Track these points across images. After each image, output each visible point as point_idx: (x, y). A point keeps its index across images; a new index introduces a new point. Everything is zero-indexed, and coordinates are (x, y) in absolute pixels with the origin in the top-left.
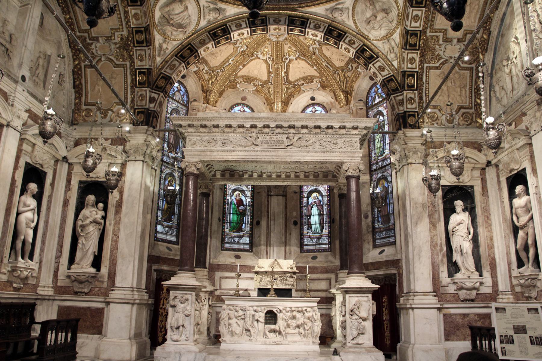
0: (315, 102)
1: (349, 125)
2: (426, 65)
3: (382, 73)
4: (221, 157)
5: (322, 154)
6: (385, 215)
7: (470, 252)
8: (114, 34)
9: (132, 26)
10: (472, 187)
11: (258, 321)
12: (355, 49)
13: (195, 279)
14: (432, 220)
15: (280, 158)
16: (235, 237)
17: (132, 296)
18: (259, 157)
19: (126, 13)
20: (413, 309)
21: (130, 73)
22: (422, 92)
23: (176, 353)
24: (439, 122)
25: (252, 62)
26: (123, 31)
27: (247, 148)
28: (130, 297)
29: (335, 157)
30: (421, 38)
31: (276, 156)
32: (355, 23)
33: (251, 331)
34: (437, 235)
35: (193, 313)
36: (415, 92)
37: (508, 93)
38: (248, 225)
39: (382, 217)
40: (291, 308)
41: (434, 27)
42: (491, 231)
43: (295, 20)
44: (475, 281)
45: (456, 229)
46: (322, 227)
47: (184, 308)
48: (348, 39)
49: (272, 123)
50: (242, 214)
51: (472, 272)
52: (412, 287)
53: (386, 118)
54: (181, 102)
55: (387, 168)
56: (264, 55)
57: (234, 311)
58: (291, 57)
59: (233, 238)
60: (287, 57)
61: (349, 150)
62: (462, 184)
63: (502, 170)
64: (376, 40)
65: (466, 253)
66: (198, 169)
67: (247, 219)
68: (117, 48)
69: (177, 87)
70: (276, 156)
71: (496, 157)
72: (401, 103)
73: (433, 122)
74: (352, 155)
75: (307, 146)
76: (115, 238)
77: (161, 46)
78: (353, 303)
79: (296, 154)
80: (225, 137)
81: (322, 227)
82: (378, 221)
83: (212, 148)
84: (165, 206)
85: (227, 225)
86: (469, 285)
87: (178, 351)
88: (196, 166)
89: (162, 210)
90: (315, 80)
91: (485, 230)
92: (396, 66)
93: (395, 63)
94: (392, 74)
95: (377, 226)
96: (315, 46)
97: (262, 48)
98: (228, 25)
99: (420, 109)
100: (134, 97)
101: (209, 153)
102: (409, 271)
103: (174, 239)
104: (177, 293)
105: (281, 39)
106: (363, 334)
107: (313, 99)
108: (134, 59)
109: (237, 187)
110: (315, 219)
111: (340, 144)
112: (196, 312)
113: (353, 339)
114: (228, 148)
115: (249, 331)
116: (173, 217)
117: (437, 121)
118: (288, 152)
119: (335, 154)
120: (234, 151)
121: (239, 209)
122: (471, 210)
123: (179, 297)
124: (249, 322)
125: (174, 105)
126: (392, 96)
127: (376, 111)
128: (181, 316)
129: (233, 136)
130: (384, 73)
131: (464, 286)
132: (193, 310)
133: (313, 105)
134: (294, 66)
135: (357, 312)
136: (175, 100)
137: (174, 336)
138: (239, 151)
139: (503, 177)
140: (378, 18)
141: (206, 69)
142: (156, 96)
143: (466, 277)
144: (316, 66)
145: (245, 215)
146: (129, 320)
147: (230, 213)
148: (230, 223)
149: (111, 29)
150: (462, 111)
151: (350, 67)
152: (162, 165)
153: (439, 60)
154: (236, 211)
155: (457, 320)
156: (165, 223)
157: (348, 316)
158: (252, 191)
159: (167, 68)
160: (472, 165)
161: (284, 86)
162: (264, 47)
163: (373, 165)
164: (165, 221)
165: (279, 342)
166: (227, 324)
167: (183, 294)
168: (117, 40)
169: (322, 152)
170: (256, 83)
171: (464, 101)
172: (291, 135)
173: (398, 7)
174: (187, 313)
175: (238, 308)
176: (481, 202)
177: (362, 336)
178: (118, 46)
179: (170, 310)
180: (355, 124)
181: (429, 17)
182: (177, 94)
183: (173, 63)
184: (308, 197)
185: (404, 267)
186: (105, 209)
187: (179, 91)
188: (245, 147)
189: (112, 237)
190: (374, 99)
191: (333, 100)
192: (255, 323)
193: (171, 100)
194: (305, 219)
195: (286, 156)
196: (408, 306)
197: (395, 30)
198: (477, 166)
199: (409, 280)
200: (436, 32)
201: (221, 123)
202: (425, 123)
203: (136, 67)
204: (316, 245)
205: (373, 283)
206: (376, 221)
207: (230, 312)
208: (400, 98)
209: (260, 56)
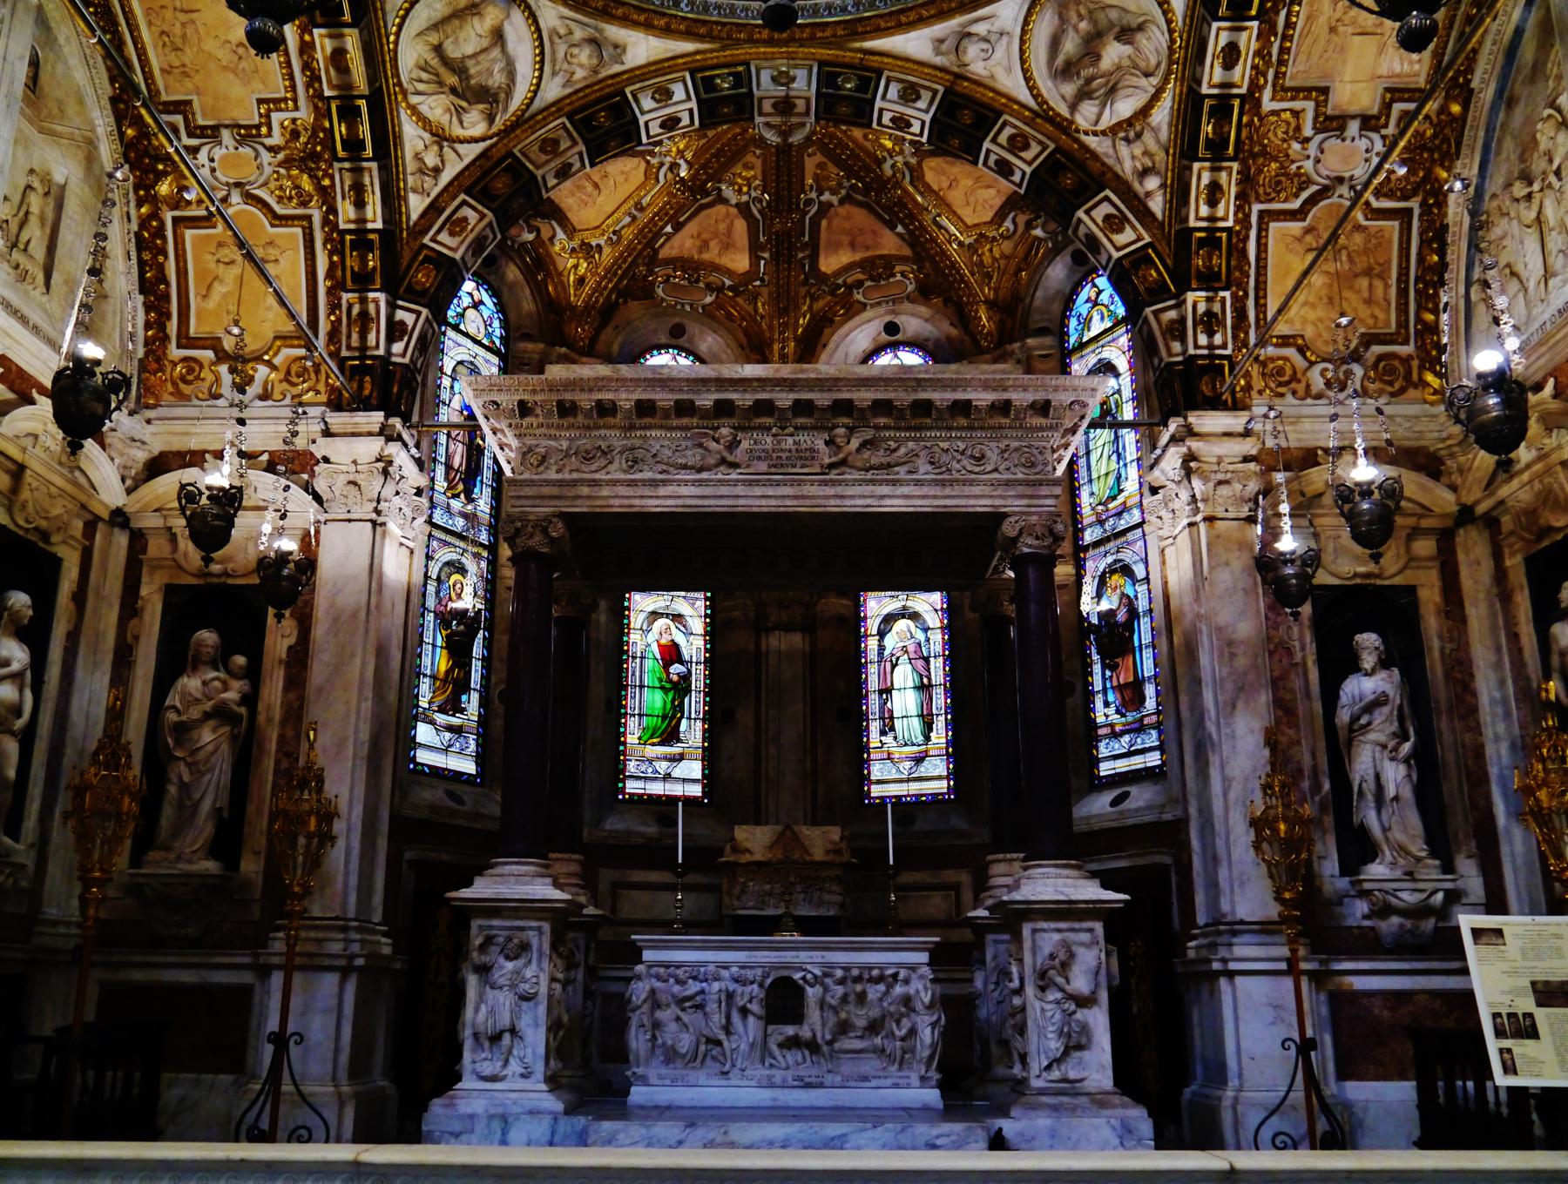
0: (899, 337)
1: (1021, 398)
2: (1256, 208)
3: (1115, 237)
4: (626, 502)
5: (937, 491)
6: (1127, 685)
7: (1407, 793)
8: (268, 116)
9: (327, 93)
10: (1411, 590)
11: (744, 1012)
12: (1029, 163)
13: (548, 880)
14: (1281, 693)
15: (808, 502)
16: (658, 759)
18: (741, 502)
20: (1231, 975)
21: (325, 245)
22: (1246, 294)
23: (491, 1117)
24: (1301, 388)
25: (705, 213)
26: (296, 108)
27: (704, 475)
29: (977, 499)
30: (1245, 119)
31: (796, 497)
32: (1028, 79)
33: (726, 1044)
34: (1299, 742)
36: (1222, 294)
37: (1531, 285)
38: (699, 724)
39: (1120, 688)
40: (847, 969)
41: (1288, 83)
42: (1477, 730)
43: (840, 74)
44: (1430, 886)
45: (1363, 721)
46: (928, 727)
47: (517, 972)
48: (1008, 131)
49: (784, 395)
50: (680, 688)
51: (1419, 860)
52: (1225, 906)
53: (1126, 383)
54: (485, 342)
55: (1130, 536)
56: (740, 191)
57: (672, 980)
58: (826, 197)
59: (650, 761)
60: (814, 195)
61: (1020, 476)
62: (1379, 582)
63: (1512, 533)
64: (1095, 134)
65: (1396, 798)
66: (553, 540)
67: (695, 703)
68: (279, 165)
69: (470, 294)
70: (796, 497)
71: (1492, 494)
72: (1177, 330)
73: (1281, 390)
74: (1029, 491)
75: (889, 466)
76: (285, 764)
77: (418, 157)
78: (1047, 951)
79: (856, 490)
80: (637, 443)
81: (928, 727)
82: (1107, 704)
83: (597, 476)
84: (443, 664)
85: (632, 724)
86: (1409, 898)
87: (500, 1110)
88: (545, 531)
89: (434, 677)
90: (898, 268)
91: (1458, 725)
92: (1159, 215)
93: (1157, 205)
94: (1148, 239)
95: (1100, 719)
96: (899, 159)
97: (738, 169)
98: (628, 91)
99: (1237, 349)
100: (339, 320)
101: (585, 491)
102: (1216, 859)
103: (469, 767)
104: (491, 927)
105: (796, 138)
106: (1080, 1047)
107: (891, 328)
108: (334, 198)
109: (662, 604)
110: (905, 702)
111: (993, 456)
113: (1048, 1068)
114: (648, 475)
115: (719, 1043)
116: (464, 698)
117: (1293, 385)
118: (833, 483)
119: (977, 490)
120: (664, 482)
121: (668, 674)
122: (1403, 653)
123: (501, 940)
124: (717, 1019)
125: (461, 350)
126: (1148, 310)
127: (1092, 360)
128: (503, 1000)
129: (659, 440)
130: (1121, 239)
131: (1394, 901)
133: (894, 346)
134: (835, 222)
135: (1060, 980)
136: (466, 335)
138: (679, 483)
139: (1513, 554)
141: (560, 235)
142: (409, 319)
143: (1398, 874)
144: (905, 226)
145: (688, 691)
147: (642, 687)
148: (640, 715)
150: (1377, 349)
151: (1008, 224)
152: (430, 535)
153: (1301, 189)
154: (661, 680)
155: (1376, 1011)
156: (441, 718)
157: (1030, 991)
158: (706, 616)
159: (439, 231)
160: (1411, 521)
161: (803, 291)
162: (740, 165)
163: (1083, 530)
164: (442, 710)
165: (813, 1080)
168: (277, 139)
169: (936, 482)
170: (714, 278)
171: (1381, 316)
172: (841, 431)
173: (1169, 22)
174: (525, 987)
175: (680, 972)
176: (1440, 637)
177: (1077, 1054)
178: (281, 156)
179: (472, 981)
180: (1040, 396)
181: (1270, 54)
182: (471, 313)
183: (459, 215)
184: (882, 634)
185: (1195, 844)
186: (254, 674)
187: (476, 305)
188: (699, 471)
189: (277, 762)
190: (1086, 322)
191: (954, 332)
192: (736, 1017)
193: (451, 333)
194: (874, 701)
195: (827, 497)
196: (1216, 966)
197: (1156, 97)
198: (1426, 523)
199: (1213, 887)
200: (1293, 99)
201: (624, 396)
202: (1254, 394)
203: (342, 226)
204: (908, 780)
205: (1105, 886)
206: (1099, 702)
207: (658, 984)
208: (1173, 314)
209: (727, 191)
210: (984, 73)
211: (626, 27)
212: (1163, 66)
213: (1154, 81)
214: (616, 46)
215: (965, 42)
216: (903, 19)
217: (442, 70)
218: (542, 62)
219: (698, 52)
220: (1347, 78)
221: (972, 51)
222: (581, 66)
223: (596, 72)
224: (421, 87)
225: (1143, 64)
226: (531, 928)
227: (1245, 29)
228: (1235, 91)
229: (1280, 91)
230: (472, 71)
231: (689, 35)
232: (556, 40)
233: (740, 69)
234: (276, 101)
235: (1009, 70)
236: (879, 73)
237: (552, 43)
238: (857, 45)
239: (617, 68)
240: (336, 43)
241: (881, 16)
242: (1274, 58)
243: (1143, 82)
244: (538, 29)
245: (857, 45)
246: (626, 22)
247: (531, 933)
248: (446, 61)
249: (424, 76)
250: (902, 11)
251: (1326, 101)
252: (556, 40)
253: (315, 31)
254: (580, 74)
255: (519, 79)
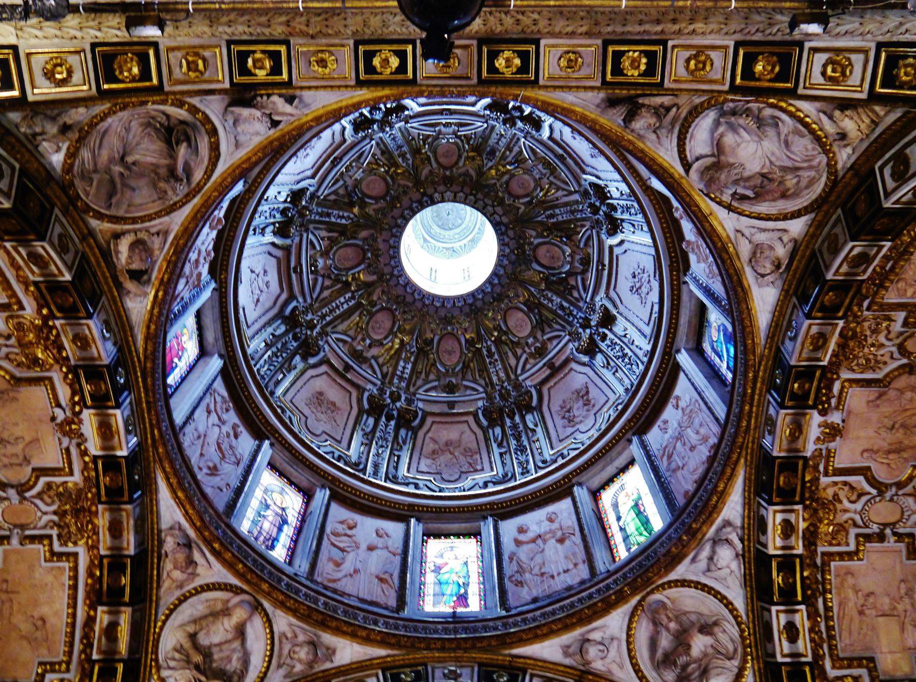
9: (95, 656)
19: (90, 621)
26: (68, 670)
140: (696, 651)
149: (40, 664)
173: (736, 617)
181: (820, 631)
210: (603, 669)
211: (337, 635)
212: (740, 650)
213: (736, 663)
214: (328, 648)
215: (586, 645)
216: (539, 632)
217: (192, 652)
218: (271, 656)
219: (389, 656)
220: (885, 650)
221: (593, 652)
222: (300, 661)
223: (311, 667)
224: (172, 664)
225: (724, 651)
227: (797, 611)
228: (803, 659)
229: (837, 661)
230: (216, 657)
231: (383, 641)
232: (284, 641)
233: (420, 668)
234: (52, 664)
235: (621, 666)
236: (524, 672)
237: (280, 642)
238: (507, 652)
239: (328, 665)
240: (113, 618)
241: (523, 631)
242: (824, 636)
243: (728, 663)
244: (272, 632)
245: (507, 652)
246: (338, 631)
248: (196, 646)
249: (177, 656)
250: (537, 627)
251: (875, 666)
252: (284, 641)
253: (100, 609)
254: (299, 668)
255: (251, 668)
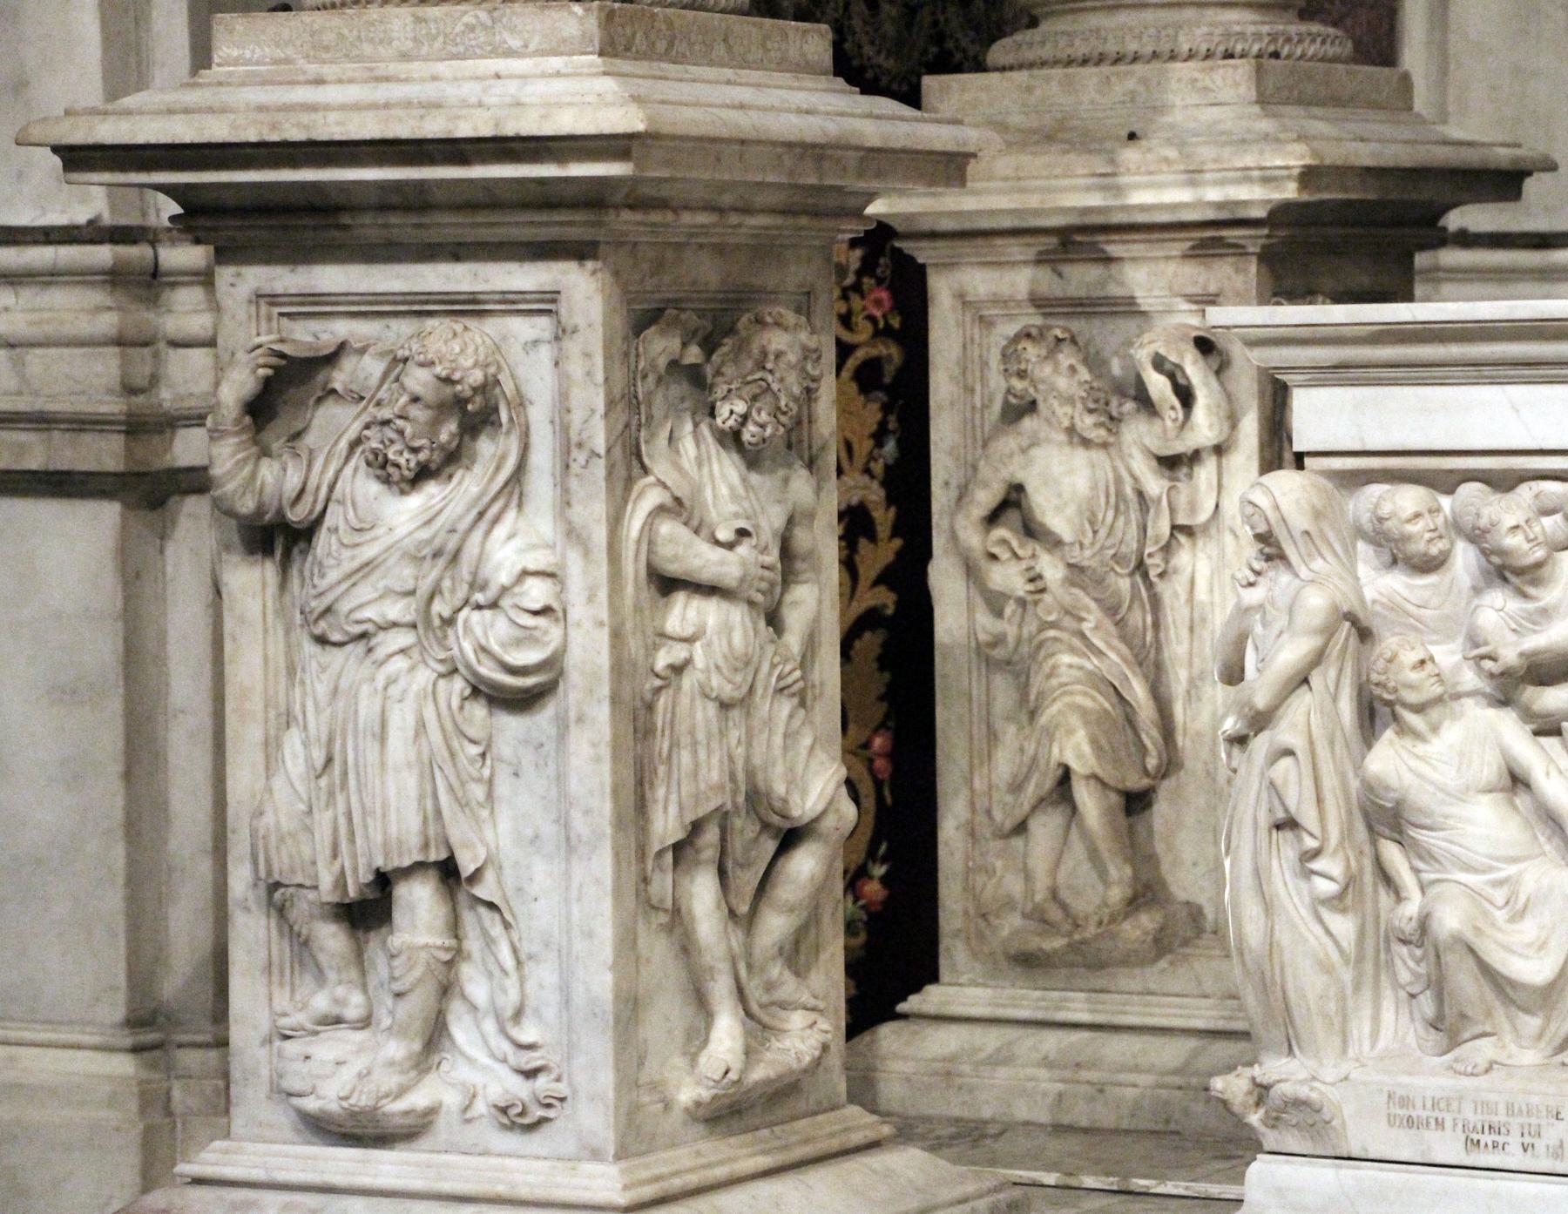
17: (104, 368)
28: (88, 380)
35: (588, 649)
57: (1464, 558)
104: (316, 305)
112: (684, 613)
123: (372, 367)
128: (400, 697)
132: (585, 582)
137: (329, 1048)
146: (109, 740)
166: (1329, 822)
167: (420, 307)
174: (489, 638)
207: (1380, 585)
226: (513, 303)
247: (522, 328)
